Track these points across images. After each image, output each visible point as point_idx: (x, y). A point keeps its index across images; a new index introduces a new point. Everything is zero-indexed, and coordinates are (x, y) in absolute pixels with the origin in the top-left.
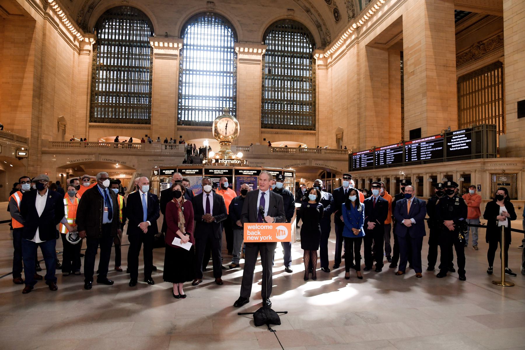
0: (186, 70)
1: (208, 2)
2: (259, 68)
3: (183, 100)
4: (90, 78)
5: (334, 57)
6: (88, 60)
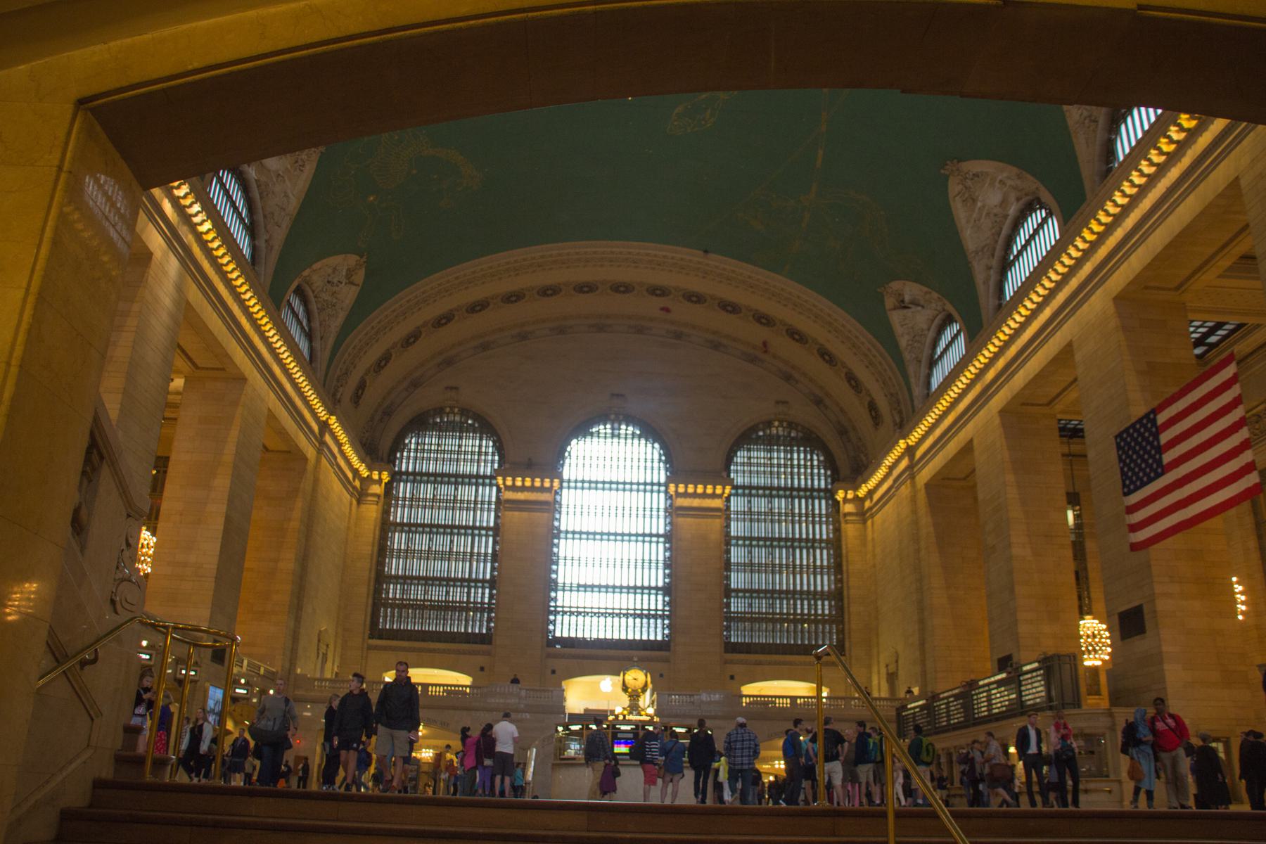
0: (567, 532)
1: (613, 395)
2: (718, 523)
3: (560, 594)
4: (376, 549)
5: (876, 497)
6: (374, 515)
